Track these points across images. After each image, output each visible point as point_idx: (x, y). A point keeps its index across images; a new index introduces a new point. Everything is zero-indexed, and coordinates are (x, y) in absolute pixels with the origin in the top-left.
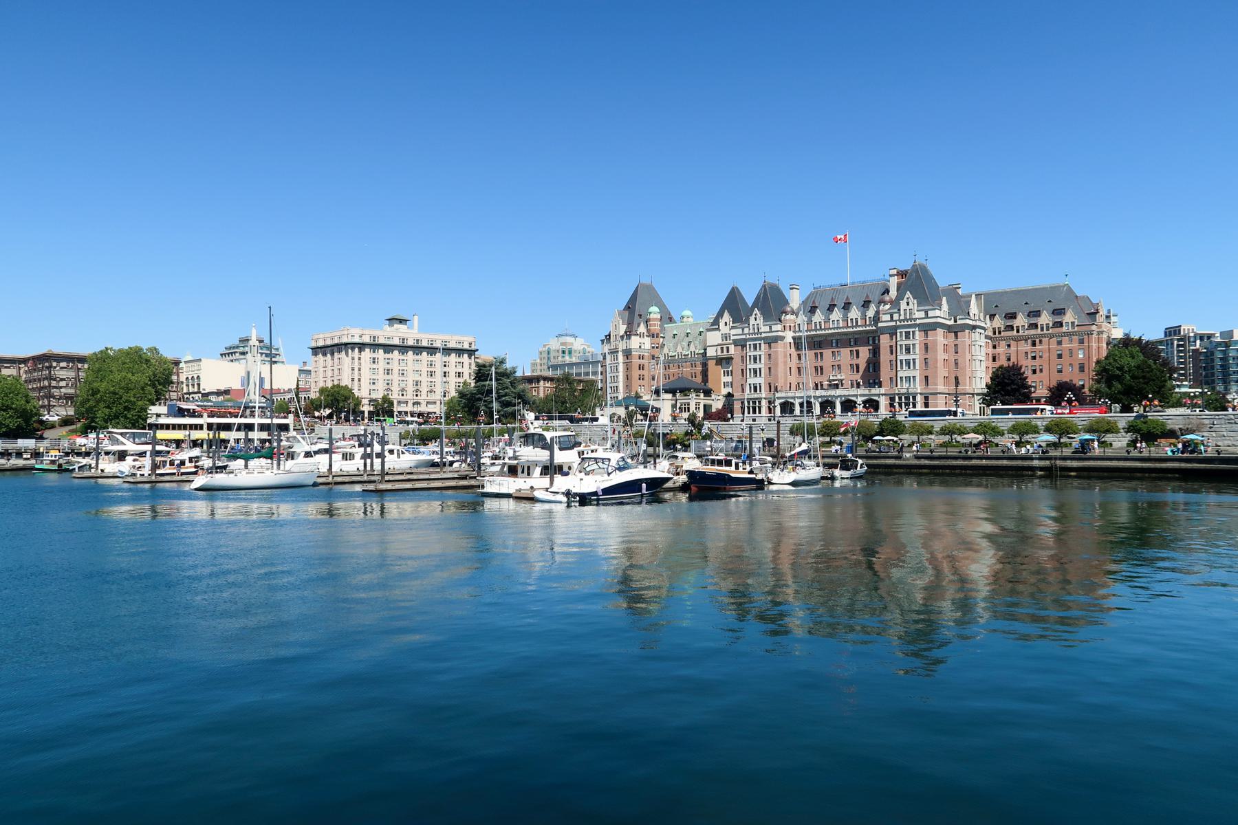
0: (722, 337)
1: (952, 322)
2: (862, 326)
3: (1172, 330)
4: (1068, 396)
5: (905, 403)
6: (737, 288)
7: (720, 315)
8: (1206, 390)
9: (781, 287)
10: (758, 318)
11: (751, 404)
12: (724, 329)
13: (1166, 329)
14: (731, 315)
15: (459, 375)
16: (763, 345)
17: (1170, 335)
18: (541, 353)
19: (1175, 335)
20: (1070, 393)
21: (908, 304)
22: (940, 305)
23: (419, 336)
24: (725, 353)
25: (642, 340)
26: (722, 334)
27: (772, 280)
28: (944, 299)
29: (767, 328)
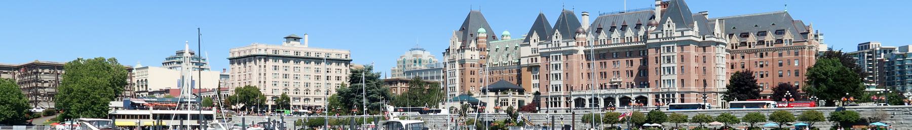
0: (532, 51)
1: (701, 40)
2: (635, 42)
3: (864, 45)
4: (786, 94)
5: (667, 99)
6: (543, 14)
7: (530, 34)
8: (888, 90)
9: (575, 14)
10: (558, 37)
11: (553, 100)
12: (533, 45)
13: (859, 45)
14: (539, 34)
15: (338, 78)
16: (562, 57)
17: (862, 49)
18: (398, 62)
19: (866, 49)
20: (788, 92)
21: (669, 26)
22: (693, 27)
23: (309, 50)
24: (534, 62)
25: (473, 53)
26: (532, 49)
27: (569, 8)
28: (696, 23)
29: (565, 45)
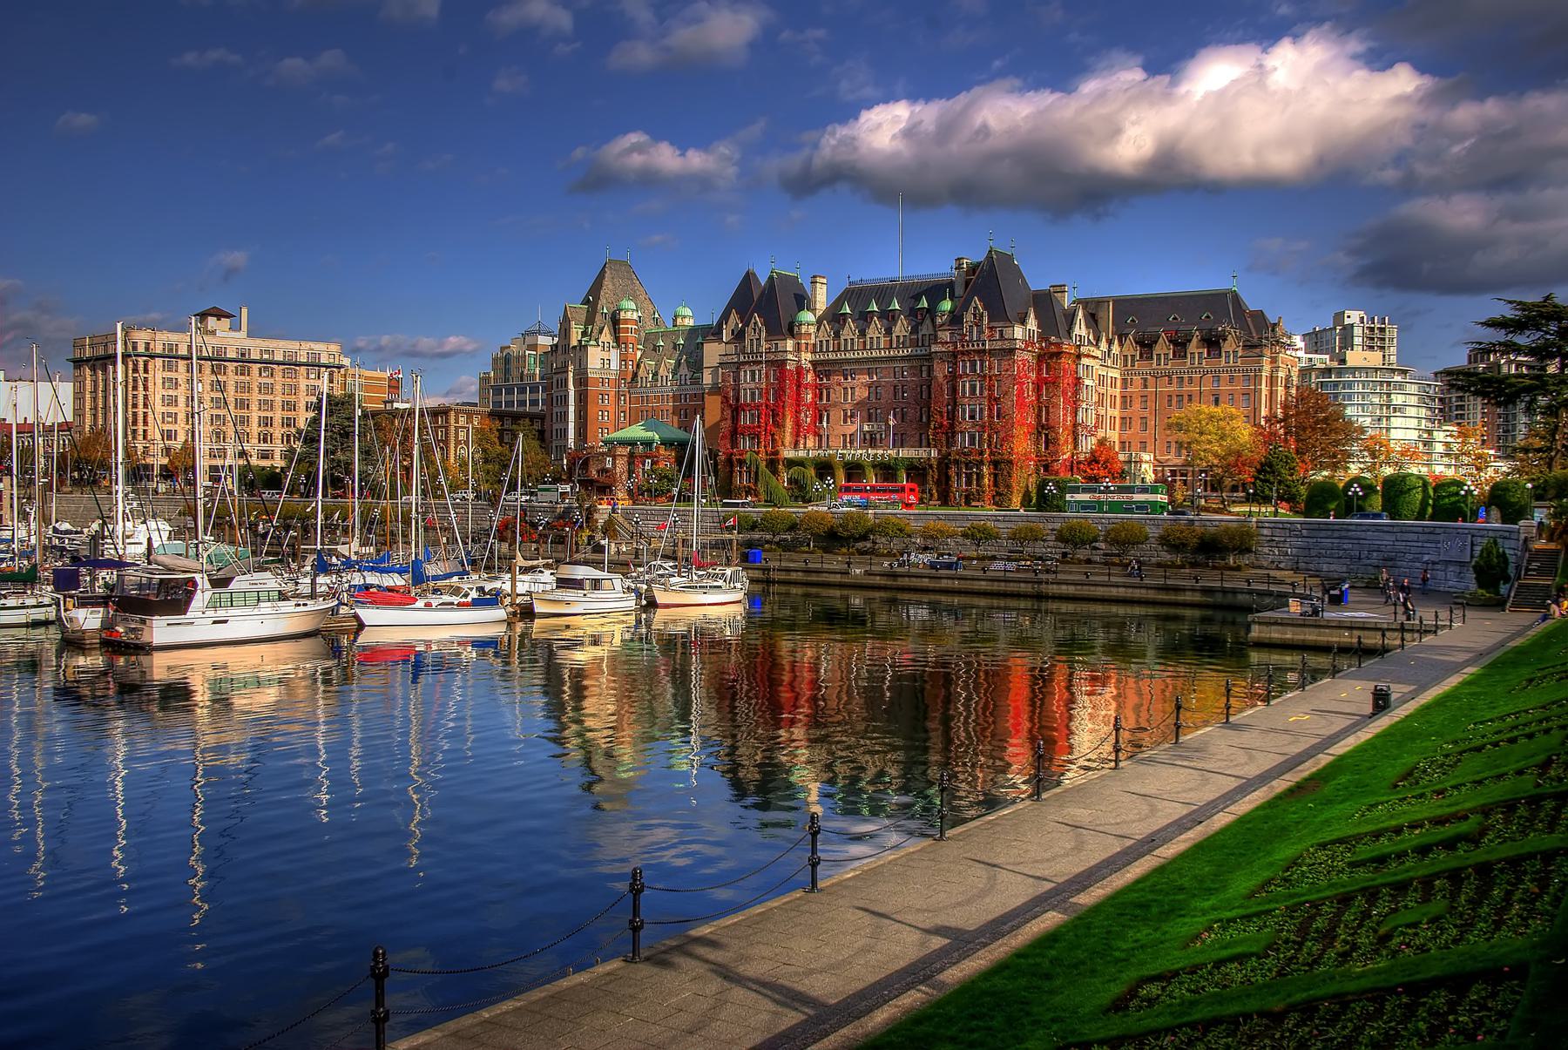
25: (605, 355)
